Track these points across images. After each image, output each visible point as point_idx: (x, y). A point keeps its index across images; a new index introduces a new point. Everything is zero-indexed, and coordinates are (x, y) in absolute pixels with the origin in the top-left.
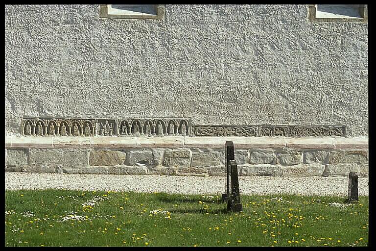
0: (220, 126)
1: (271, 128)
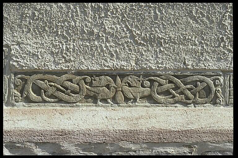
0: (99, 74)
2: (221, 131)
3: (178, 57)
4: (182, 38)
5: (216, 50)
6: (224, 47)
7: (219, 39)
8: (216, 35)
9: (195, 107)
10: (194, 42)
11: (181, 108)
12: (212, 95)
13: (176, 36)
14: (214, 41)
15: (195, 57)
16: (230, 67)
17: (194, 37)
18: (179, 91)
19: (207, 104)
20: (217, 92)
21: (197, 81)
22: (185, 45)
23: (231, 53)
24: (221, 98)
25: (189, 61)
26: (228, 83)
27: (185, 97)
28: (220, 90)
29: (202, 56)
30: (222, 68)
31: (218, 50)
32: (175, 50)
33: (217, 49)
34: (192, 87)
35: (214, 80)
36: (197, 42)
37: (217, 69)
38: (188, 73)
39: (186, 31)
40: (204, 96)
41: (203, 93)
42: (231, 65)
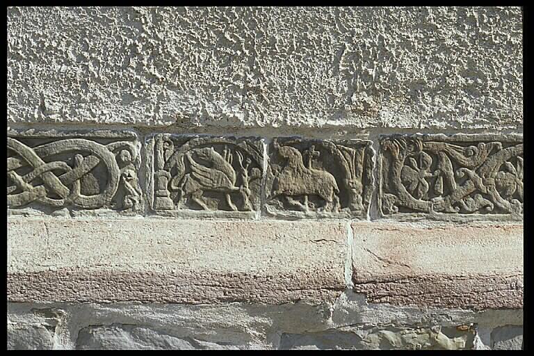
1: (242, 148)
2: (123, 274)
3: (26, 93)
4: (35, 44)
5: (119, 75)
6: (139, 68)
7: (126, 48)
8: (119, 38)
9: (73, 216)
10: (64, 56)
11: (38, 218)
12: (112, 186)
13: (20, 41)
14: (114, 54)
15: (68, 93)
16: (154, 117)
17: (63, 44)
18: (32, 175)
19: (102, 210)
20: (124, 179)
21: (75, 152)
22: (44, 62)
23: (158, 84)
24: (136, 194)
25: (54, 101)
26: (151, 158)
27: (47, 192)
28: (133, 173)
29: (84, 91)
30: (134, 119)
31: (124, 76)
32: (19, 75)
33: (121, 74)
34: (62, 166)
35: (117, 151)
36: (71, 56)
37: (123, 122)
38: (51, 132)
39: (44, 29)
40: (95, 188)
41: (91, 182)
42: (157, 115)
